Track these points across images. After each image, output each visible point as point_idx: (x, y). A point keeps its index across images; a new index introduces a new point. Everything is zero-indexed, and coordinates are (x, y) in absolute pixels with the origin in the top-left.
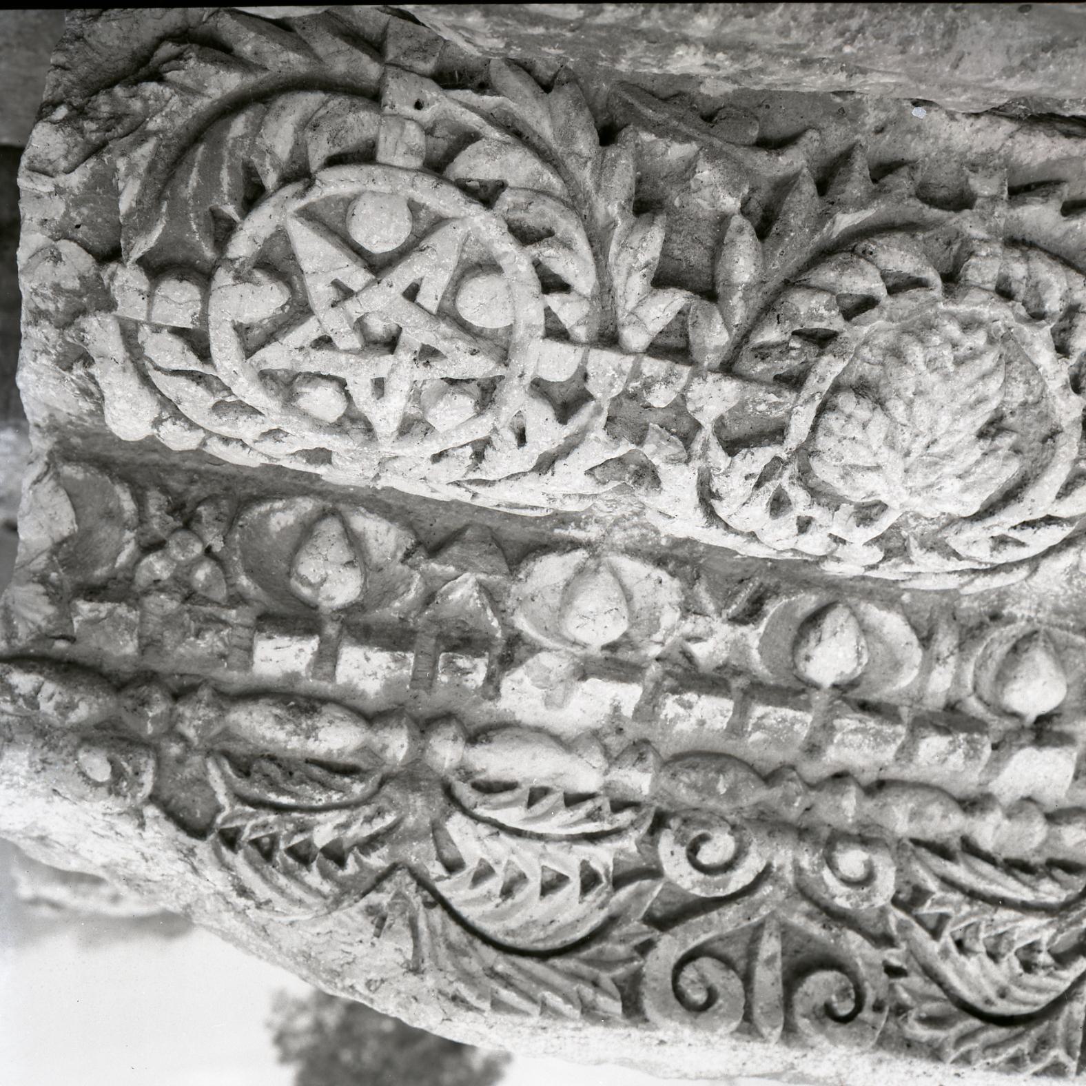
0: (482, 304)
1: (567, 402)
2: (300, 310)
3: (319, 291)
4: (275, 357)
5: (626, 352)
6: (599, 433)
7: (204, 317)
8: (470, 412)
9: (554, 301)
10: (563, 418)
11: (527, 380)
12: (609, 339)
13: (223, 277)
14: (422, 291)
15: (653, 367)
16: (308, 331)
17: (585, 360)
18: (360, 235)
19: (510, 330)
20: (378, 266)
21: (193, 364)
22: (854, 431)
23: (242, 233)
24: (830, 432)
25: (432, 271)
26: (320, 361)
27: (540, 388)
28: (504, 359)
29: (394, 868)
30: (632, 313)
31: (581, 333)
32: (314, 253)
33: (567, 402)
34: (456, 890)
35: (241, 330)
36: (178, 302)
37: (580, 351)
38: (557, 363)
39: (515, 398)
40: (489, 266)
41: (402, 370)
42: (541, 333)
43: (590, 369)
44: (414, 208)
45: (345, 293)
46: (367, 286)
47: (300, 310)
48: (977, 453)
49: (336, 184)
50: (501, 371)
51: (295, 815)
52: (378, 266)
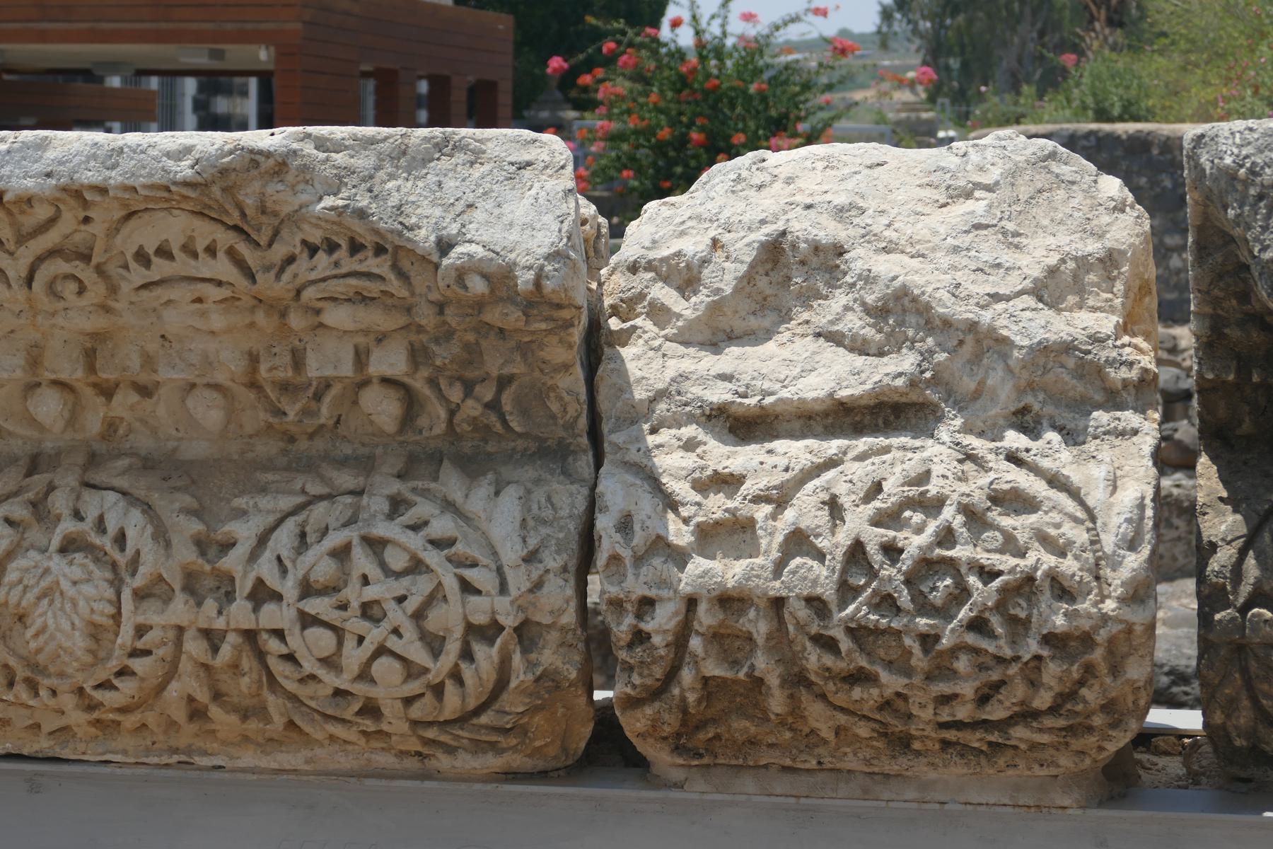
0: (323, 640)
1: (261, 594)
2: (418, 616)
3: (409, 631)
5: (235, 630)
6: (238, 573)
7: (464, 604)
9: (284, 650)
10: (260, 582)
12: (250, 636)
13: (458, 632)
14: (355, 643)
15: (220, 624)
16: (412, 604)
17: (257, 620)
18: (397, 665)
19: (304, 628)
20: (381, 651)
21: (469, 574)
22: (95, 606)
24: (110, 601)
25: (353, 657)
26: (400, 586)
27: (278, 597)
29: (270, 245)
30: (241, 651)
31: (265, 636)
32: (418, 654)
33: (261, 594)
34: (225, 238)
38: (271, 615)
39: (289, 588)
40: (325, 662)
41: (354, 594)
43: (253, 617)
44: (373, 681)
45: (396, 632)
46: (385, 640)
47: (418, 616)
48: (24, 603)
49: (414, 687)
50: (301, 605)
51: (343, 270)
52: (381, 651)
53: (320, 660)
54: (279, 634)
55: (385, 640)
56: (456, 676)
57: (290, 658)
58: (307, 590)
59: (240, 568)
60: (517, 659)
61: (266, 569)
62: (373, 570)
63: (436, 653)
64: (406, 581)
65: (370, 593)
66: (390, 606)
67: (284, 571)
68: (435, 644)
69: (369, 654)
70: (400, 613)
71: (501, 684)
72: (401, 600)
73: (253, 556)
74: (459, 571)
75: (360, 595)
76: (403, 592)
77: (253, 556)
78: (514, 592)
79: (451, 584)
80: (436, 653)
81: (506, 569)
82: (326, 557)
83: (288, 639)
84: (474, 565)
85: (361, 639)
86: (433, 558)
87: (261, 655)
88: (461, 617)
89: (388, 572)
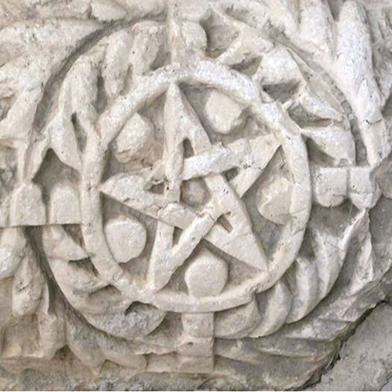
2: (249, 198)
4: (259, 152)
8: (121, 146)
9: (80, 255)
10: (50, 155)
11: (83, 184)
16: (244, 181)
19: (105, 222)
20: (203, 246)
21: (319, 135)
23: (294, 252)
25: (166, 253)
28: (104, 199)
33: (49, 172)
35: (284, 170)
36: (331, 182)
37: (52, 221)
42: (84, 229)
43: (42, 209)
46: (208, 234)
47: (249, 198)
53: (121, 265)
54: (72, 230)
55: (208, 234)
56: (288, 277)
57: (85, 264)
58: (110, 166)
59: (23, 134)
60: (367, 248)
61: (57, 134)
62: (195, 133)
63: (268, 248)
64: (237, 146)
65: (195, 165)
66: (217, 184)
67: (81, 142)
68: (266, 234)
69: (190, 253)
70: (231, 195)
71: (340, 283)
72: (230, 174)
73: (39, 120)
74: (307, 131)
75: (182, 169)
76: (234, 164)
77: (39, 120)
78: (373, 159)
79: (296, 152)
80: (268, 248)
81: (363, 126)
82: (137, 117)
83: (86, 238)
84: (320, 122)
85: (177, 232)
86: (271, 112)
87: (42, 262)
88: (308, 198)
89: (214, 136)
